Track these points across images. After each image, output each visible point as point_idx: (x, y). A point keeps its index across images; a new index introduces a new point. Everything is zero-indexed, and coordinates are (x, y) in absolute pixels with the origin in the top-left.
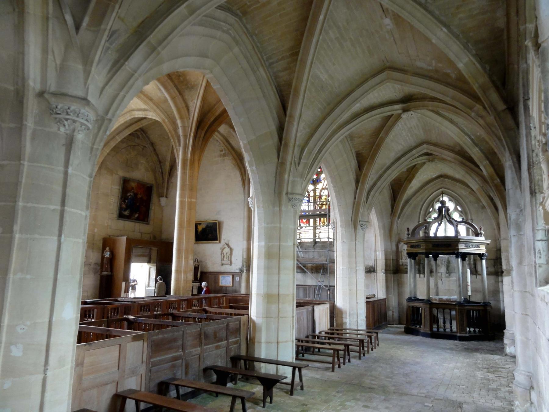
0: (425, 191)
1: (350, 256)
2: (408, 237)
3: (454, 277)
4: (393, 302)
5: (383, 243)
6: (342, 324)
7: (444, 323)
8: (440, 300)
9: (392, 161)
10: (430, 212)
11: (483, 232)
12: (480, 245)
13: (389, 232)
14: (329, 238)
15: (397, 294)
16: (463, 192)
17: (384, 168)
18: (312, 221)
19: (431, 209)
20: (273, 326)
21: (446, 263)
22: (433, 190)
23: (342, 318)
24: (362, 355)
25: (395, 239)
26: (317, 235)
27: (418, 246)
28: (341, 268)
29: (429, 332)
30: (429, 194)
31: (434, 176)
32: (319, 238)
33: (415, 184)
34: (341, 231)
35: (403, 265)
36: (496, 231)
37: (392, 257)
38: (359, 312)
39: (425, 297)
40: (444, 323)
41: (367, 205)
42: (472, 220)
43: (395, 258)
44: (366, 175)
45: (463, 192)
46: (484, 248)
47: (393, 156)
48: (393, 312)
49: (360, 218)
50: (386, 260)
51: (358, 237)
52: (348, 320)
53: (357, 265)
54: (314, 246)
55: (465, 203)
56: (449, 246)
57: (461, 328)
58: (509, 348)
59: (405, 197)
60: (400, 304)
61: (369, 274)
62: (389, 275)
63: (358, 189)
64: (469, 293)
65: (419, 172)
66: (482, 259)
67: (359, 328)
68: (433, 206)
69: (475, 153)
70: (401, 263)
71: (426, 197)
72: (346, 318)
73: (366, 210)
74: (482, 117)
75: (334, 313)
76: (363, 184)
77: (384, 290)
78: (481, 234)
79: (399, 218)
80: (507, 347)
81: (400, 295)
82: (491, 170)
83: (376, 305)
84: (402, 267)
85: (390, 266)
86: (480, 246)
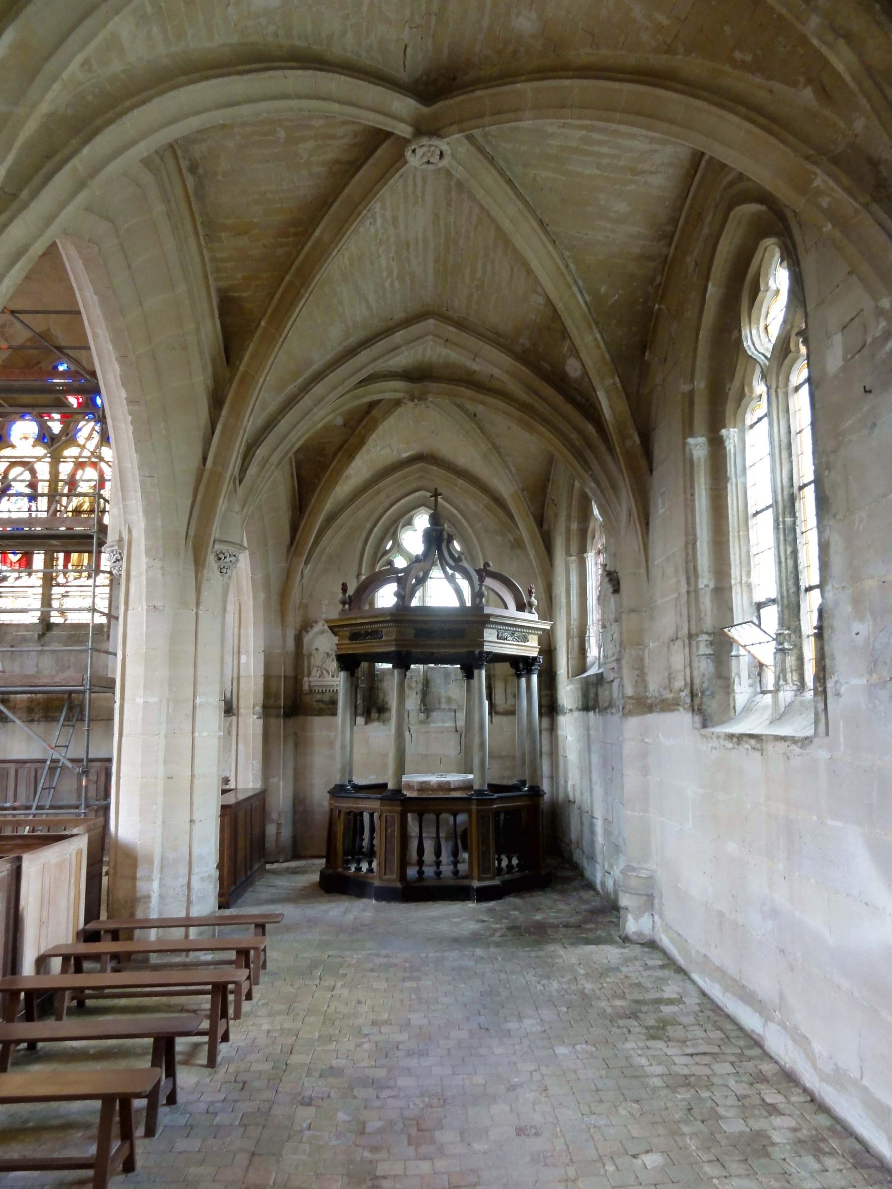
0: (378, 492)
1: (173, 660)
2: (343, 610)
3: (442, 721)
4: (281, 799)
5: (261, 631)
6: (133, 901)
8: (424, 787)
9: (329, 357)
10: (386, 552)
11: (535, 602)
13: (281, 598)
14: (93, 610)
15: (290, 773)
16: (470, 503)
17: (307, 375)
18: (38, 560)
19: (390, 543)
21: (420, 686)
22: (399, 494)
23: (134, 878)
25: (294, 620)
26: (55, 604)
27: (374, 634)
28: (140, 700)
29: (399, 885)
30: (387, 503)
31: (405, 455)
32: (62, 612)
33: (359, 469)
34: (149, 568)
37: (283, 669)
38: (196, 851)
40: (438, 853)
41: (240, 491)
43: (290, 673)
44: (248, 382)
46: (536, 644)
47: (335, 337)
48: (279, 825)
49: (216, 533)
50: (267, 678)
51: (205, 594)
52: (155, 885)
53: (200, 689)
54: (41, 636)
55: (474, 531)
58: (636, 919)
59: (329, 505)
60: (300, 804)
61: (291, 721)
62: (273, 721)
63: (219, 427)
65: (380, 429)
66: (530, 672)
67: (195, 912)
68: (395, 538)
70: (306, 687)
71: (380, 510)
72: (150, 879)
73: (237, 508)
74: (848, 37)
75: (106, 862)
76: (237, 413)
77: (256, 765)
78: (531, 605)
79: (307, 562)
80: (630, 917)
81: (300, 775)
82: (623, 406)
83: (241, 814)
84: (307, 699)
85: (277, 696)
86: (530, 637)
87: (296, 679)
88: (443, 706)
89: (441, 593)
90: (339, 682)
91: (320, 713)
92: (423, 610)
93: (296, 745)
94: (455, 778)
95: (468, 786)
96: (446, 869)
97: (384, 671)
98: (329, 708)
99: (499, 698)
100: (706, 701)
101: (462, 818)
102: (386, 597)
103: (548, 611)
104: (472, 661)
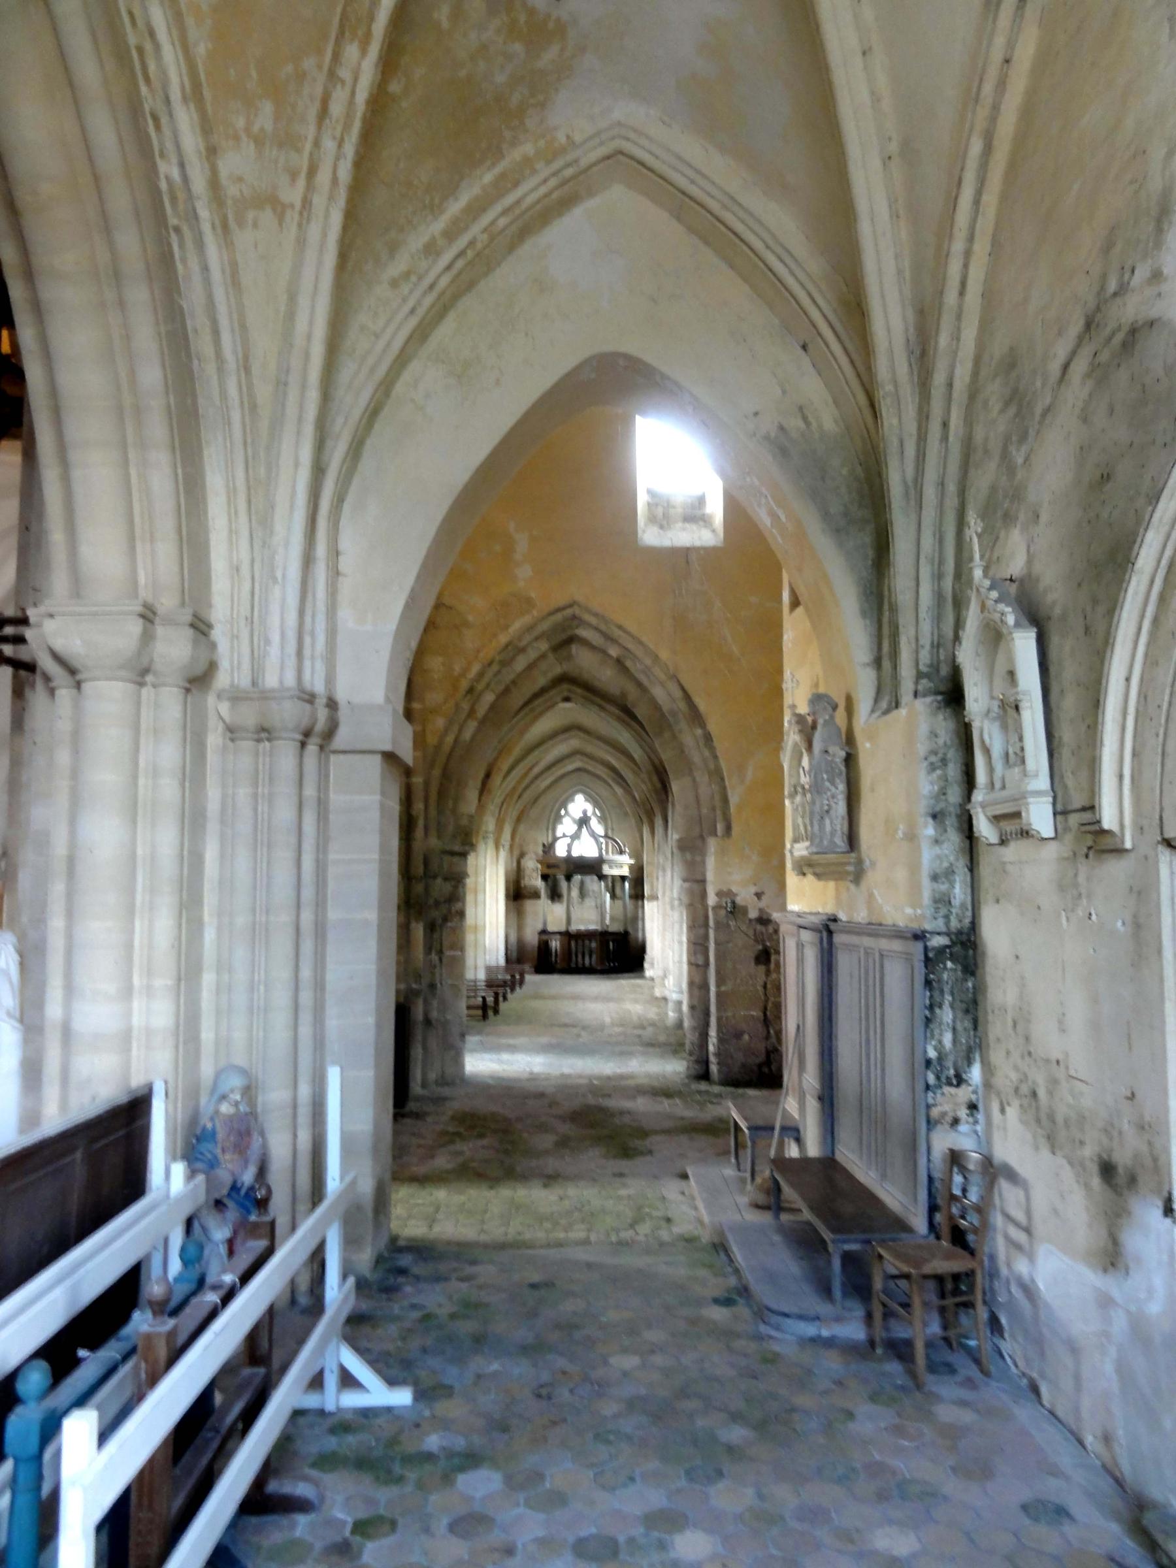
3: (589, 902)
12: (621, 865)
24: (501, 999)
25: (516, 853)
37: (513, 877)
39: (563, 929)
45: (605, 793)
56: (592, 867)
57: (601, 960)
64: (607, 922)
89: (586, 848)
90: (539, 884)
94: (592, 927)
98: (536, 895)
99: (618, 891)
102: (561, 851)
104: (602, 877)
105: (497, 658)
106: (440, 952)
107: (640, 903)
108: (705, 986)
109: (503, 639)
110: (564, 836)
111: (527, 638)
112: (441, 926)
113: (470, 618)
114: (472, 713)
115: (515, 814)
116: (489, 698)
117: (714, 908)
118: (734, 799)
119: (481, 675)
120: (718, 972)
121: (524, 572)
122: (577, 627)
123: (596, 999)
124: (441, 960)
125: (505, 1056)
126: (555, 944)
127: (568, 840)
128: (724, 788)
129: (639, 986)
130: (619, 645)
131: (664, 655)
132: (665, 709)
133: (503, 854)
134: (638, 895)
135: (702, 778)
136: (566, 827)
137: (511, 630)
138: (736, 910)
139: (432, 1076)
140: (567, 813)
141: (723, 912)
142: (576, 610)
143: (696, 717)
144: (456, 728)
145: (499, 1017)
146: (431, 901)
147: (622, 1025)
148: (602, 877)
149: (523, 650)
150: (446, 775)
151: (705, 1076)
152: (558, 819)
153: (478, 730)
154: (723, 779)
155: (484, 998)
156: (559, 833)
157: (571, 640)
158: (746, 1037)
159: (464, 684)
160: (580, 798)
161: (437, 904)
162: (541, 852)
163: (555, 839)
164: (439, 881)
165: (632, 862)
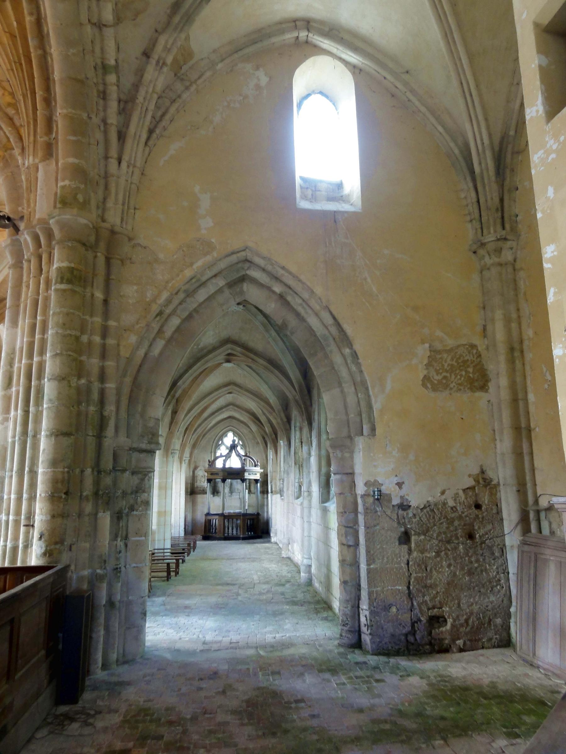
3: (235, 496)
7: (233, 529)
8: (229, 513)
16: (245, 430)
20: (162, 530)
25: (192, 466)
27: (217, 474)
35: (197, 487)
36: (265, 461)
39: (220, 512)
40: (233, 529)
42: (249, 452)
45: (245, 431)
56: (237, 474)
69: (263, 419)
87: (193, 484)
88: (236, 491)
89: (235, 463)
91: (200, 494)
92: (230, 468)
93: (193, 503)
95: (240, 513)
96: (235, 532)
97: (218, 481)
98: (204, 492)
99: (252, 489)
100: (281, 492)
101: (239, 522)
102: (219, 464)
103: (264, 467)
104: (243, 480)
105: (183, 288)
106: (126, 537)
107: (265, 496)
108: (356, 564)
109: (188, 273)
110: (221, 456)
111: (209, 274)
112: (127, 515)
113: (161, 256)
114: (160, 331)
115: (192, 442)
116: (175, 322)
117: (362, 496)
118: (377, 406)
119: (169, 301)
120: (368, 552)
121: (206, 223)
122: (249, 268)
123: (244, 559)
124: (126, 545)
125: (182, 620)
126: (216, 521)
127: (224, 458)
128: (369, 396)
129: (269, 548)
130: (281, 282)
131: (319, 290)
132: (318, 334)
133: (184, 466)
134: (265, 491)
135: (349, 389)
136: (223, 451)
137: (195, 266)
138: (380, 498)
139: (114, 656)
140: (223, 443)
141: (371, 500)
142: (249, 255)
143: (344, 339)
144: (146, 344)
145: (178, 577)
146: (119, 493)
147: (267, 583)
148: (243, 480)
149: (203, 284)
150: (135, 383)
151: (358, 645)
152: (217, 446)
153: (166, 346)
154: (367, 389)
155: (168, 564)
156: (218, 454)
157: (243, 279)
158: (394, 609)
159: (155, 308)
160: (230, 435)
161: (124, 494)
162: (207, 466)
163: (216, 458)
164: (127, 474)
165: (262, 471)
